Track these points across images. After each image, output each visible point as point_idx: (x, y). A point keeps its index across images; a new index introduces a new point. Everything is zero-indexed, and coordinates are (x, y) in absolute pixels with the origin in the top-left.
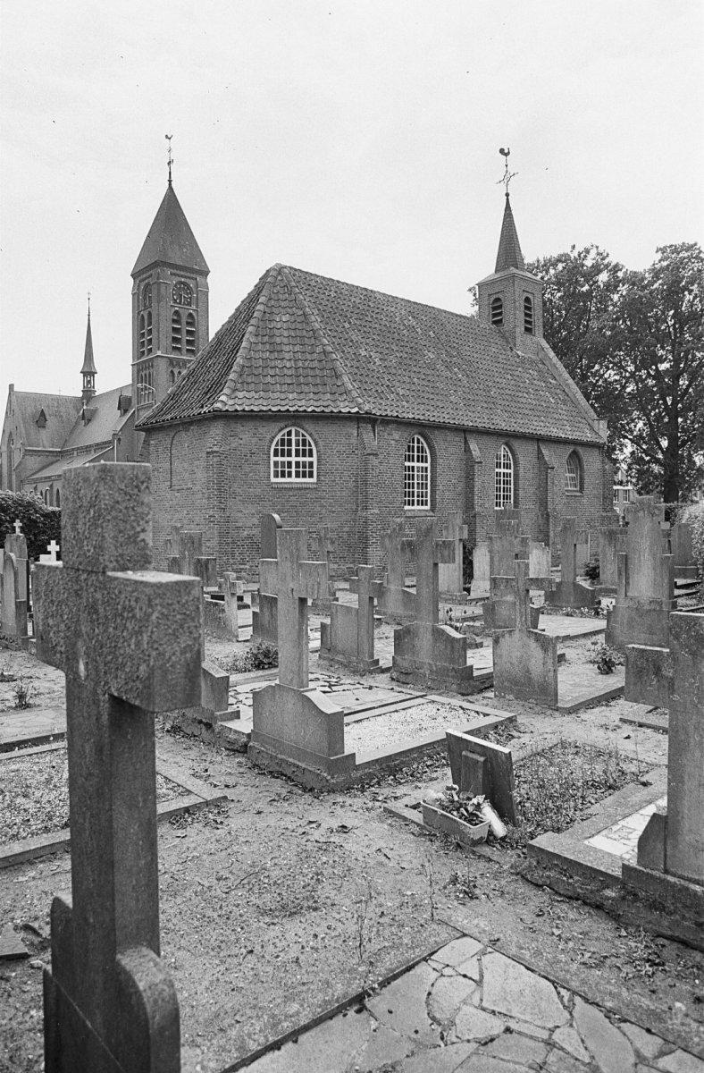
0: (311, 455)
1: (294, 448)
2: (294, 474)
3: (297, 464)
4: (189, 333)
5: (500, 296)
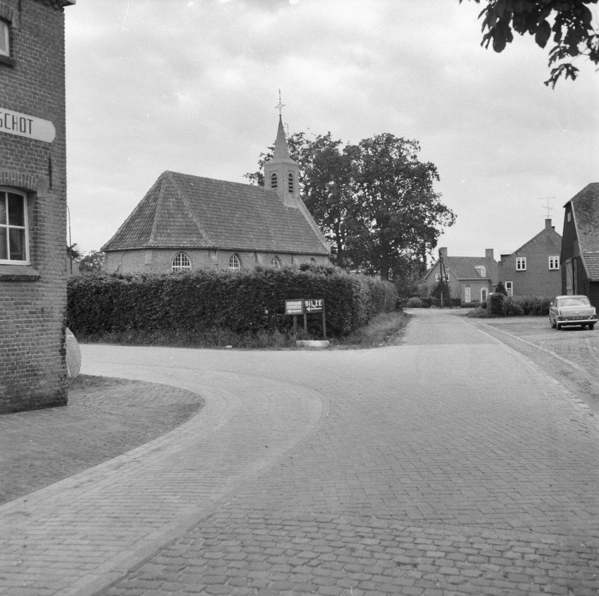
0: (189, 265)
1: (181, 262)
5: (275, 173)
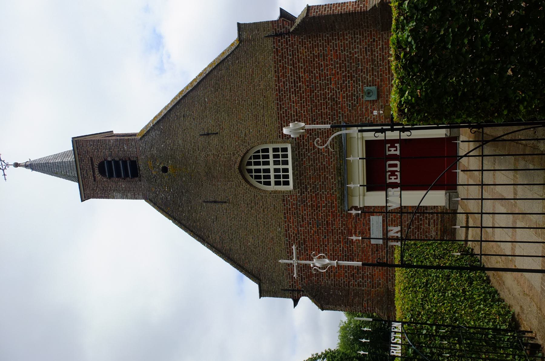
0: (267, 150)
1: (262, 167)
2: (285, 167)
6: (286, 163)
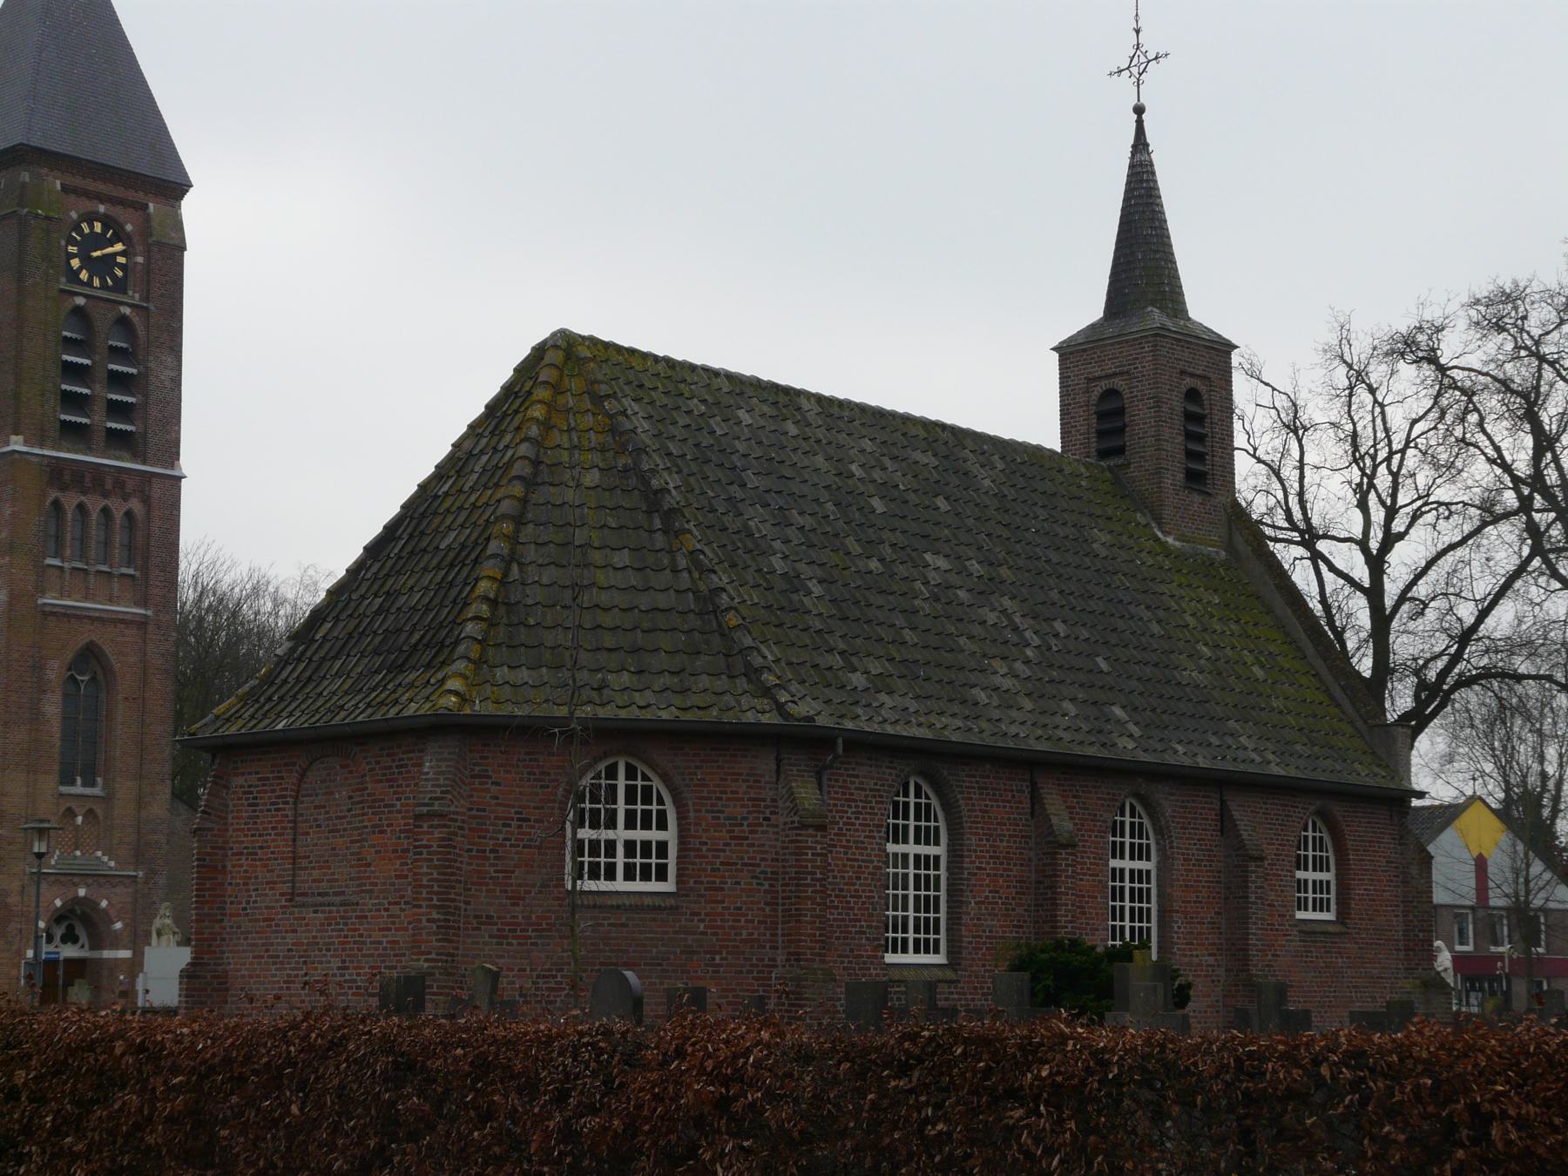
0: (662, 826)
1: (621, 807)
3: (630, 846)
4: (118, 380)
5: (1119, 383)
6: (629, 875)
